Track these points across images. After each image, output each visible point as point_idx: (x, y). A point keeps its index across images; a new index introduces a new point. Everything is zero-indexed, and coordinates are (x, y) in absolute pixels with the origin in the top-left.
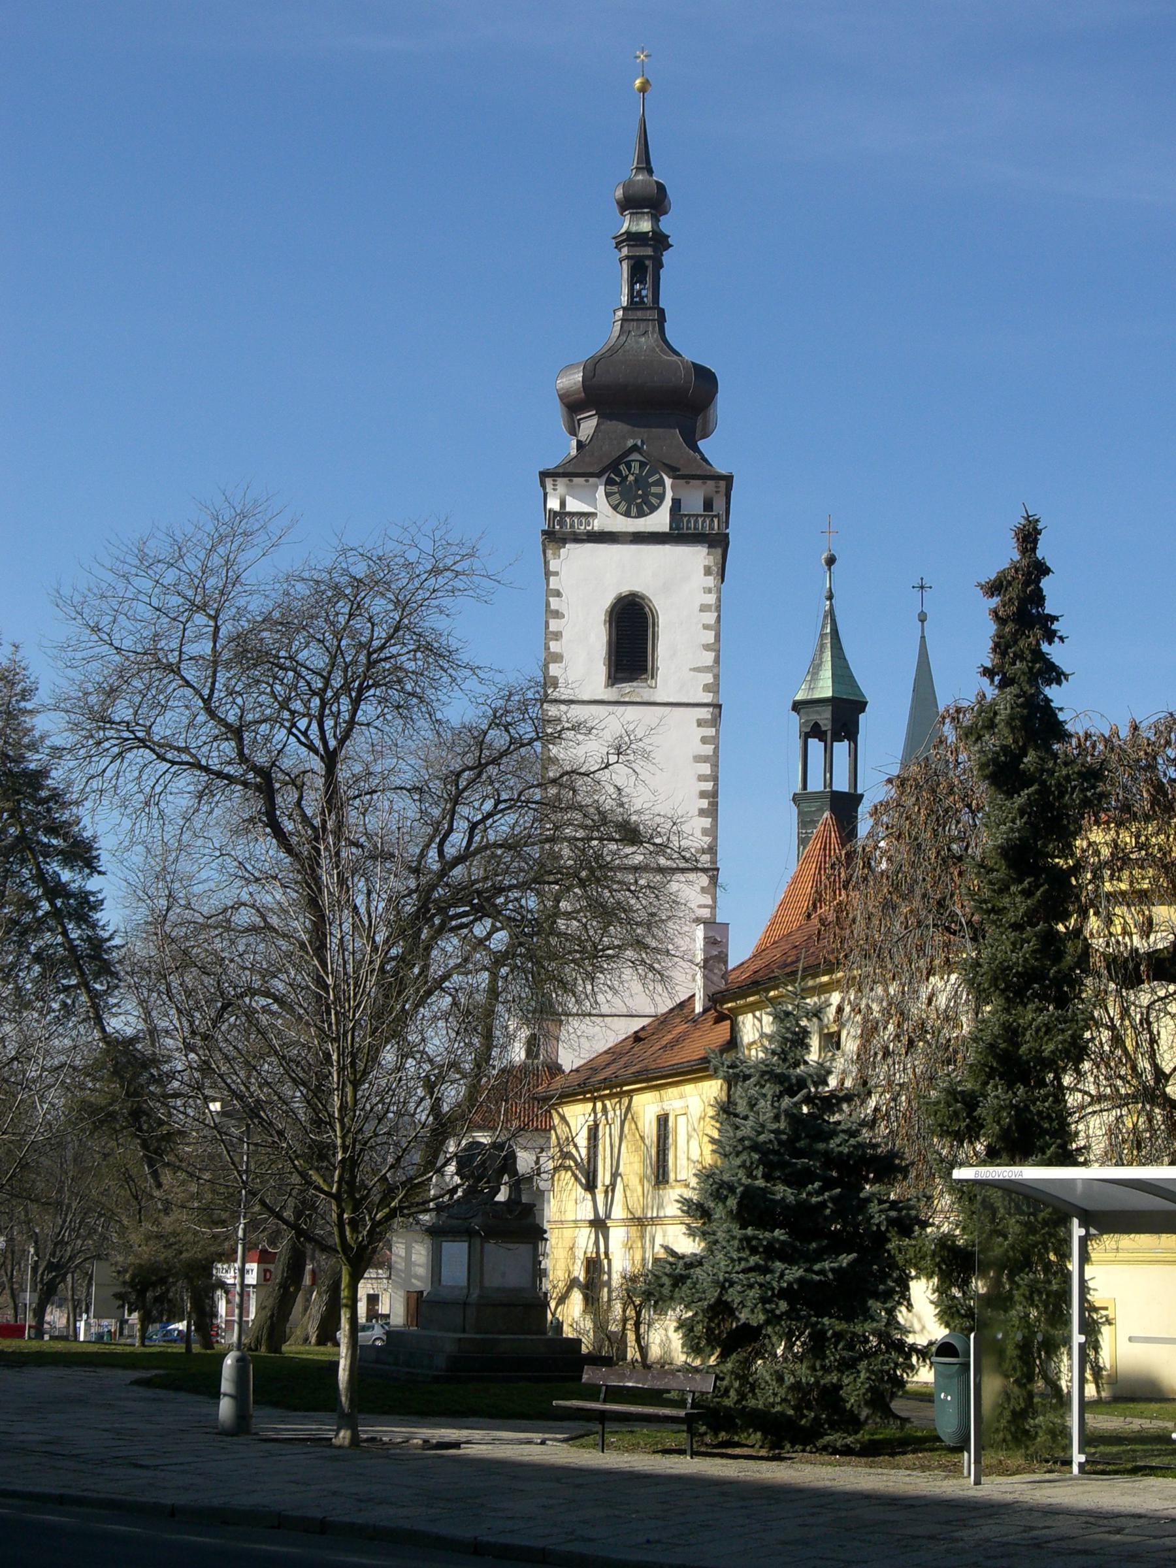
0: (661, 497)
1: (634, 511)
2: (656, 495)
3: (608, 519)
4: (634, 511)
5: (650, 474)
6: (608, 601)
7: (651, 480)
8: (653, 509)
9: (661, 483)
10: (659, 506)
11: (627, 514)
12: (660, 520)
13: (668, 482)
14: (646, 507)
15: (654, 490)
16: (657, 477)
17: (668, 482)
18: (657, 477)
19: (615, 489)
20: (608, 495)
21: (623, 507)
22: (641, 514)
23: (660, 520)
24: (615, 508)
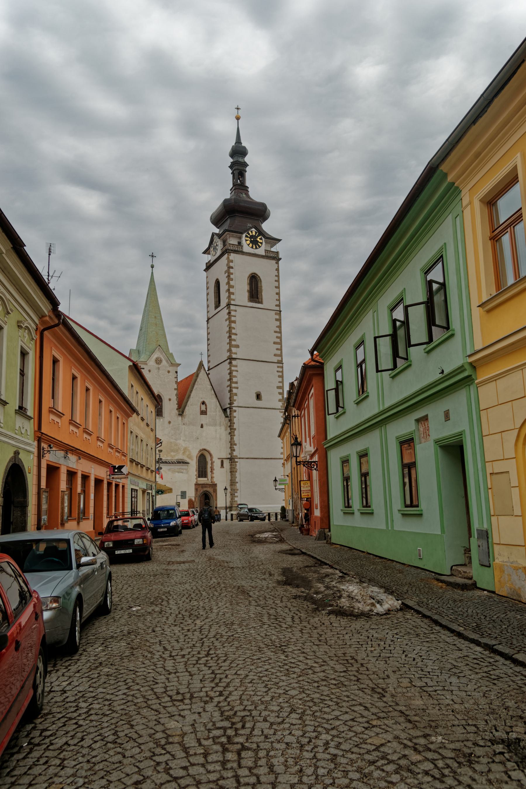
0: (261, 243)
1: (254, 247)
2: (260, 243)
4: (254, 247)
5: (258, 236)
6: (247, 275)
8: (260, 247)
11: (252, 247)
12: (261, 251)
13: (263, 239)
19: (248, 239)
20: (246, 240)
22: (256, 248)
23: (261, 251)
24: (249, 245)
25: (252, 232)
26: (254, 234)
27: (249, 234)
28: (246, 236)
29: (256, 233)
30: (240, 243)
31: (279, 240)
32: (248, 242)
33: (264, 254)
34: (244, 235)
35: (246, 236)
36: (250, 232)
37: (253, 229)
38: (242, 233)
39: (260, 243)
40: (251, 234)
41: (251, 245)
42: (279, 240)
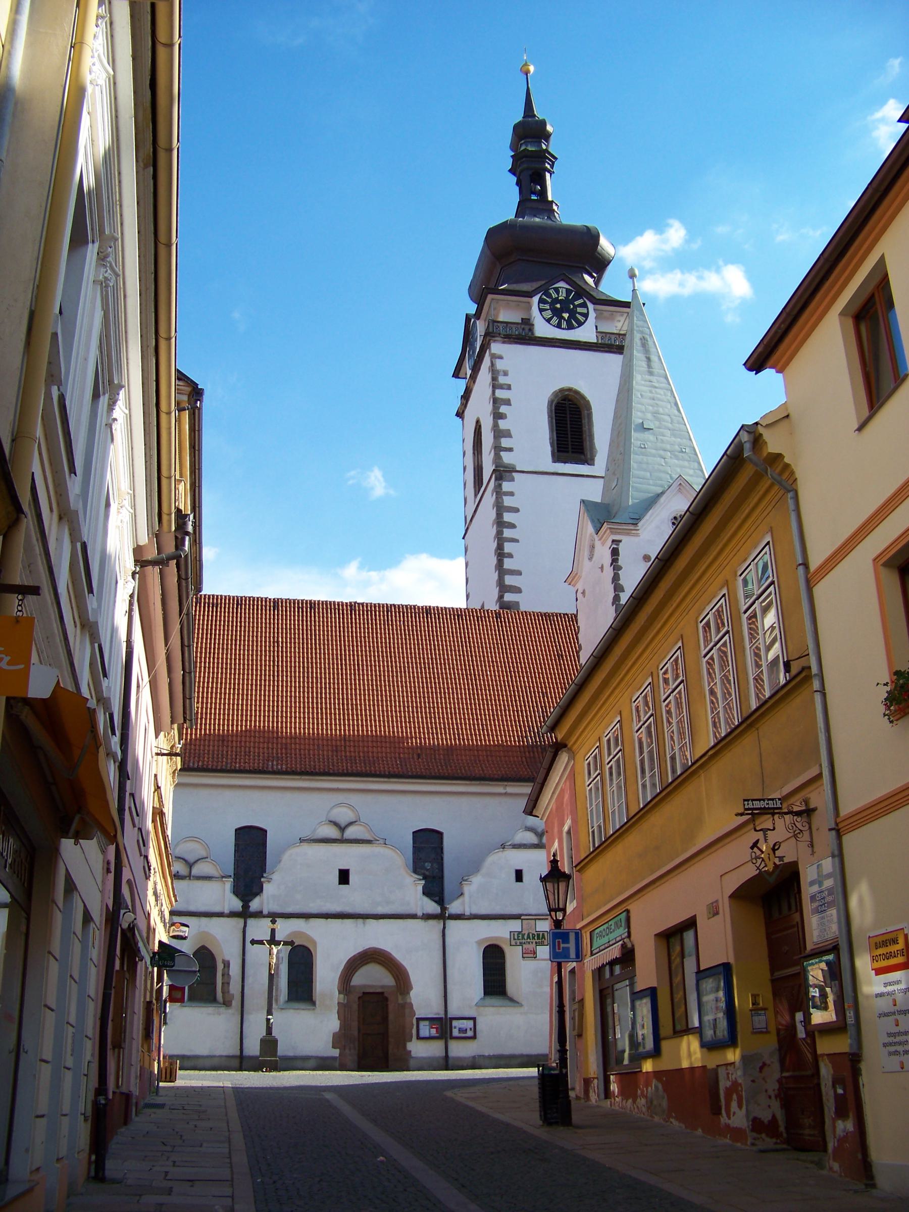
0: (586, 316)
1: (564, 325)
2: (581, 314)
3: (542, 329)
4: (564, 325)
7: (576, 303)
8: (580, 324)
9: (584, 305)
10: (585, 322)
11: (559, 326)
13: (590, 306)
15: (579, 310)
16: (581, 301)
17: (590, 306)
18: (581, 301)
20: (541, 310)
21: (555, 320)
22: (570, 327)
23: (586, 333)
24: (548, 321)
25: (557, 290)
27: (549, 296)
29: (568, 292)
32: (548, 314)
34: (536, 299)
35: (541, 301)
36: (551, 291)
37: (562, 284)
38: (530, 295)
39: (581, 314)
40: (554, 295)
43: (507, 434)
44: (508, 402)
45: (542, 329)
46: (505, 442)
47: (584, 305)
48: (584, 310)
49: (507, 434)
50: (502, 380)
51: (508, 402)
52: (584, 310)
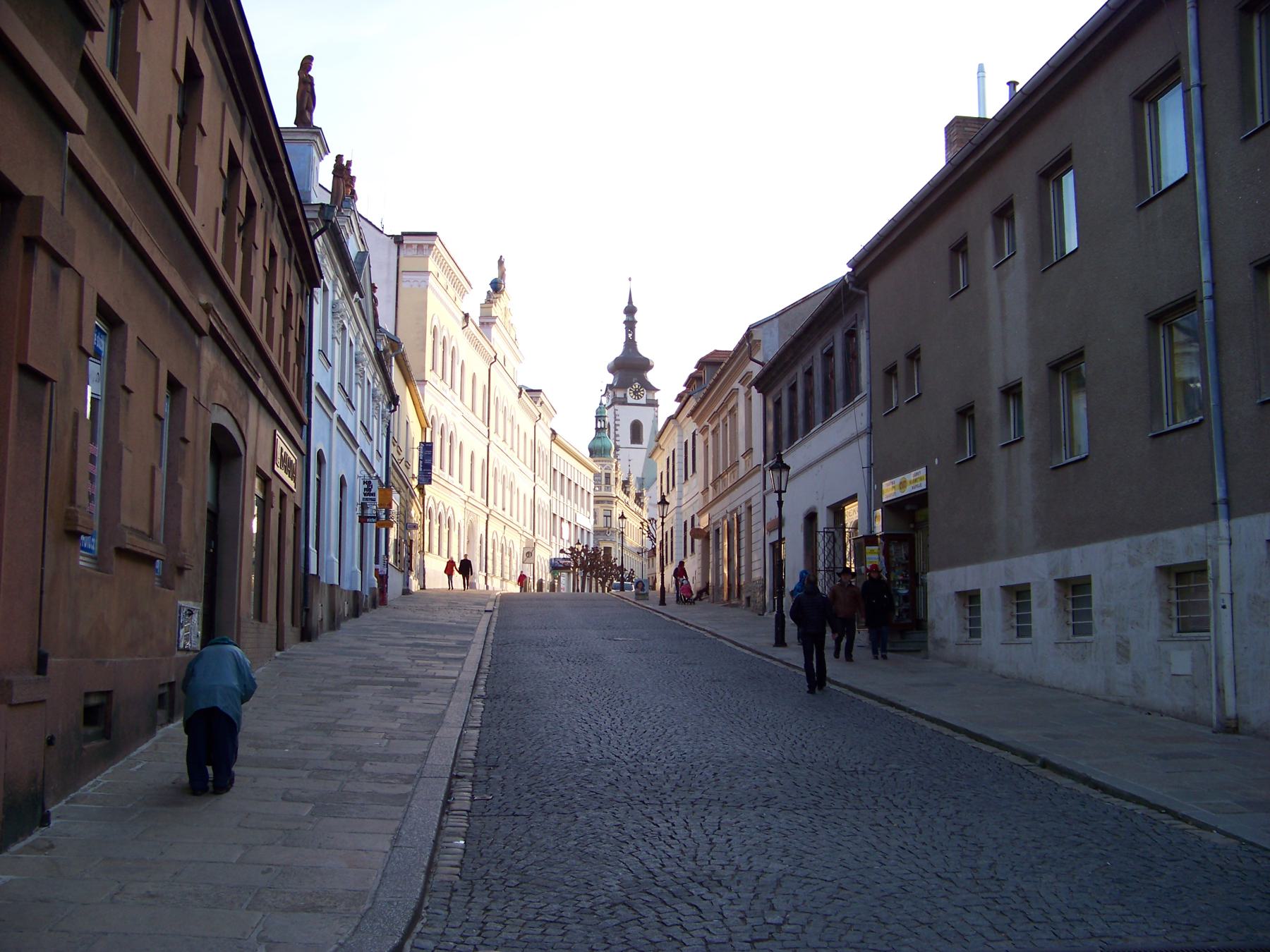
0: (643, 394)
11: (635, 399)
12: (643, 401)
14: (639, 397)
21: (634, 397)
22: (638, 399)
23: (643, 401)
26: (637, 387)
28: (630, 390)
30: (625, 395)
31: (658, 390)
32: (632, 394)
33: (645, 403)
34: (628, 390)
35: (630, 390)
37: (637, 383)
41: (634, 397)
42: (658, 390)
43: (618, 436)
44: (618, 425)
45: (630, 400)
46: (617, 438)
47: (643, 391)
48: (642, 392)
49: (618, 436)
50: (617, 418)
51: (618, 425)
52: (642, 392)
